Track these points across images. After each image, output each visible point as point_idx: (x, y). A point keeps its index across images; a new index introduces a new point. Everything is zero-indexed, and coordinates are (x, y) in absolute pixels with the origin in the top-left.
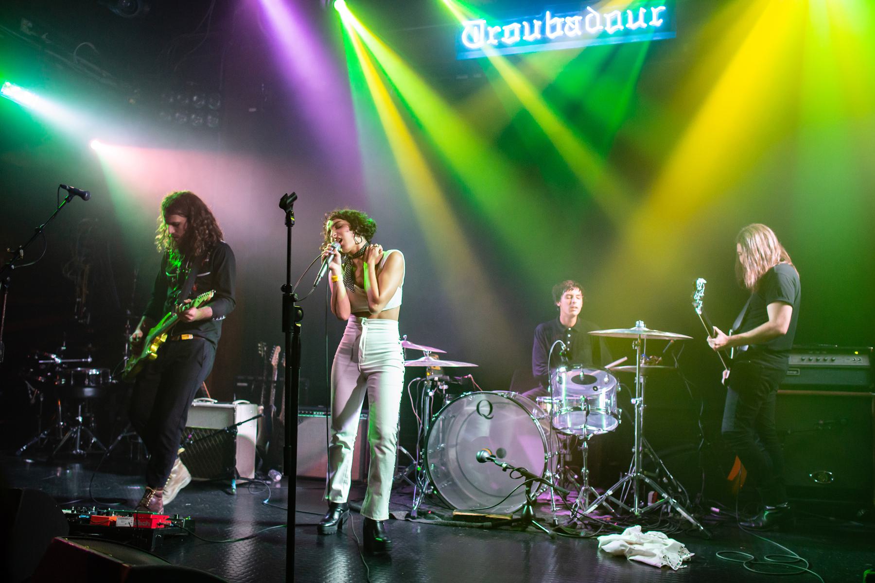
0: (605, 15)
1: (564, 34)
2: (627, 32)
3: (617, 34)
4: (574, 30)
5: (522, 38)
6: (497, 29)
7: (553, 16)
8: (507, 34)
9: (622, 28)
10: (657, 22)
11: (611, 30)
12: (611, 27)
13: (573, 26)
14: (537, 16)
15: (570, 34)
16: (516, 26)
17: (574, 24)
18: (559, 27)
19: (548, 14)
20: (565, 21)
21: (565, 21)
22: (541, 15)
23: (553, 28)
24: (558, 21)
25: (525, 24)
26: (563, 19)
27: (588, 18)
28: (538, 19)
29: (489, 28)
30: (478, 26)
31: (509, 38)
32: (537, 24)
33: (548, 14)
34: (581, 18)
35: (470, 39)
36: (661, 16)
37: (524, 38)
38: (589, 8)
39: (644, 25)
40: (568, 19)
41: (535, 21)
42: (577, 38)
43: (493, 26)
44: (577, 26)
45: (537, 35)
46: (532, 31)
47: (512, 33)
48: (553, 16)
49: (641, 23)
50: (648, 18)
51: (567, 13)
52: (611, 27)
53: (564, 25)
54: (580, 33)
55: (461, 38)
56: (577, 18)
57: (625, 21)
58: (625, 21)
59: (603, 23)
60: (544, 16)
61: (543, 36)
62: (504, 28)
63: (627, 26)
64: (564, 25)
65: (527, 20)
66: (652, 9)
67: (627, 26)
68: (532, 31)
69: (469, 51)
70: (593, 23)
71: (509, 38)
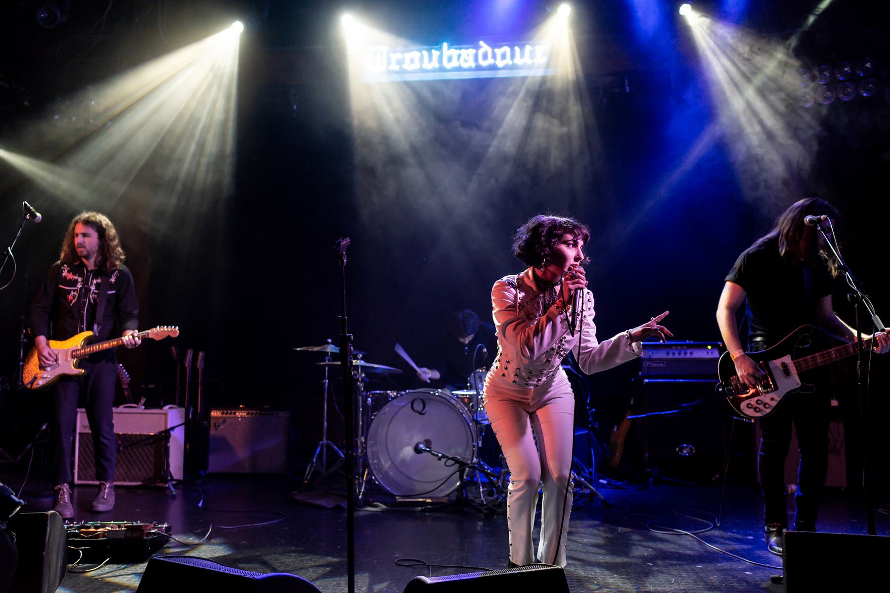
0: (496, 50)
1: (460, 65)
2: (513, 67)
3: (506, 68)
4: (468, 62)
5: (421, 66)
6: (399, 56)
7: (449, 48)
8: (407, 61)
11: (500, 63)
14: (435, 47)
15: (465, 65)
16: (416, 54)
17: (468, 55)
18: (455, 58)
19: (445, 45)
20: (460, 54)
21: (460, 54)
22: (439, 46)
23: (450, 59)
24: (454, 52)
25: (425, 53)
26: (458, 51)
27: (481, 52)
28: (436, 49)
29: (391, 55)
32: (435, 53)
33: (445, 45)
34: (474, 51)
38: (481, 43)
39: (530, 62)
40: (463, 50)
41: (433, 51)
42: (470, 69)
43: (395, 52)
45: (435, 64)
47: (412, 61)
48: (449, 48)
52: (501, 61)
53: (459, 56)
54: (473, 65)
56: (472, 52)
57: (513, 56)
59: (494, 56)
63: (516, 61)
64: (459, 56)
65: (425, 50)
67: (516, 61)
70: (485, 57)
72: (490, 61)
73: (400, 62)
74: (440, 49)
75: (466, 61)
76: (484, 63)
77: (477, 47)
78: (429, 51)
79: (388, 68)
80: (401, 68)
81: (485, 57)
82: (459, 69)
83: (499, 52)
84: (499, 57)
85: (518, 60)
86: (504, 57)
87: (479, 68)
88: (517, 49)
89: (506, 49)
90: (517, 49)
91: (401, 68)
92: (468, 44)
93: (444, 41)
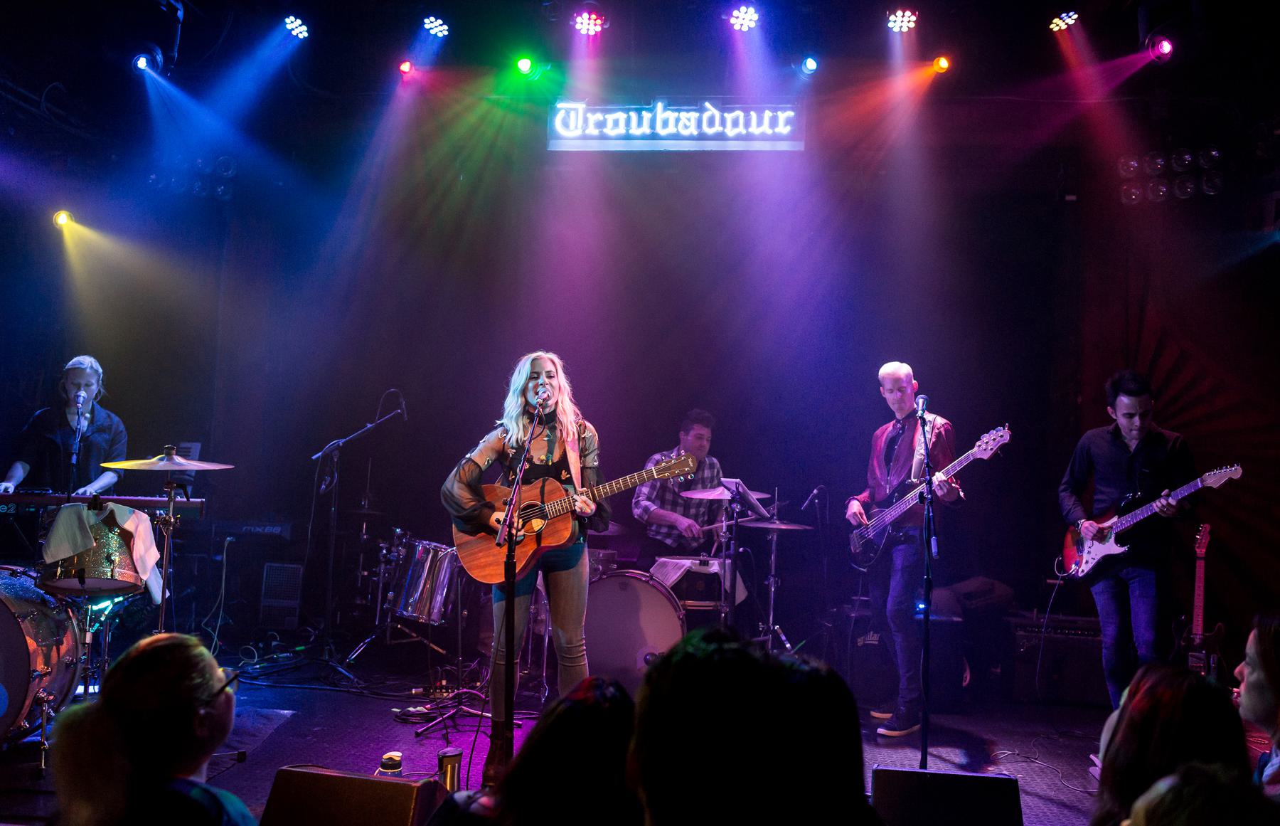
0: (726, 115)
1: (678, 131)
2: (749, 137)
3: (739, 138)
5: (628, 131)
6: (599, 116)
7: (665, 109)
8: (610, 123)
9: (744, 132)
10: (783, 129)
11: (730, 132)
12: (731, 130)
13: (688, 124)
14: (647, 107)
15: (685, 133)
16: (621, 116)
18: (672, 122)
19: (660, 106)
23: (665, 124)
24: (671, 115)
25: (633, 115)
26: (676, 114)
27: (706, 116)
28: (646, 110)
29: (589, 115)
30: (576, 110)
31: (613, 129)
32: (646, 116)
33: (660, 106)
35: (566, 124)
36: (788, 122)
37: (631, 132)
38: (707, 104)
39: (770, 132)
40: (683, 115)
41: (644, 113)
42: (691, 138)
43: (594, 112)
44: (693, 124)
45: (646, 129)
46: (640, 124)
47: (616, 123)
48: (665, 109)
49: (766, 129)
50: (774, 122)
51: (682, 108)
52: (731, 130)
53: (678, 120)
54: (695, 133)
55: (554, 121)
56: (696, 115)
57: (747, 124)
58: (747, 124)
59: (723, 123)
60: (654, 107)
61: (653, 131)
62: (607, 116)
63: (751, 130)
64: (678, 120)
66: (779, 113)
67: (751, 130)
68: (640, 124)
69: (561, 139)
70: (711, 122)
71: (613, 129)
72: (717, 128)
73: (601, 125)
74: (651, 110)
75: (686, 127)
76: (710, 131)
77: (702, 110)
78: (639, 111)
79: (584, 131)
80: (601, 132)
81: (711, 122)
82: (677, 137)
83: (729, 117)
84: (729, 124)
85: (754, 130)
86: (735, 123)
87: (702, 137)
88: (753, 115)
89: (739, 114)
90: (753, 115)
91: (601, 132)
92: (689, 104)
93: (661, 99)
